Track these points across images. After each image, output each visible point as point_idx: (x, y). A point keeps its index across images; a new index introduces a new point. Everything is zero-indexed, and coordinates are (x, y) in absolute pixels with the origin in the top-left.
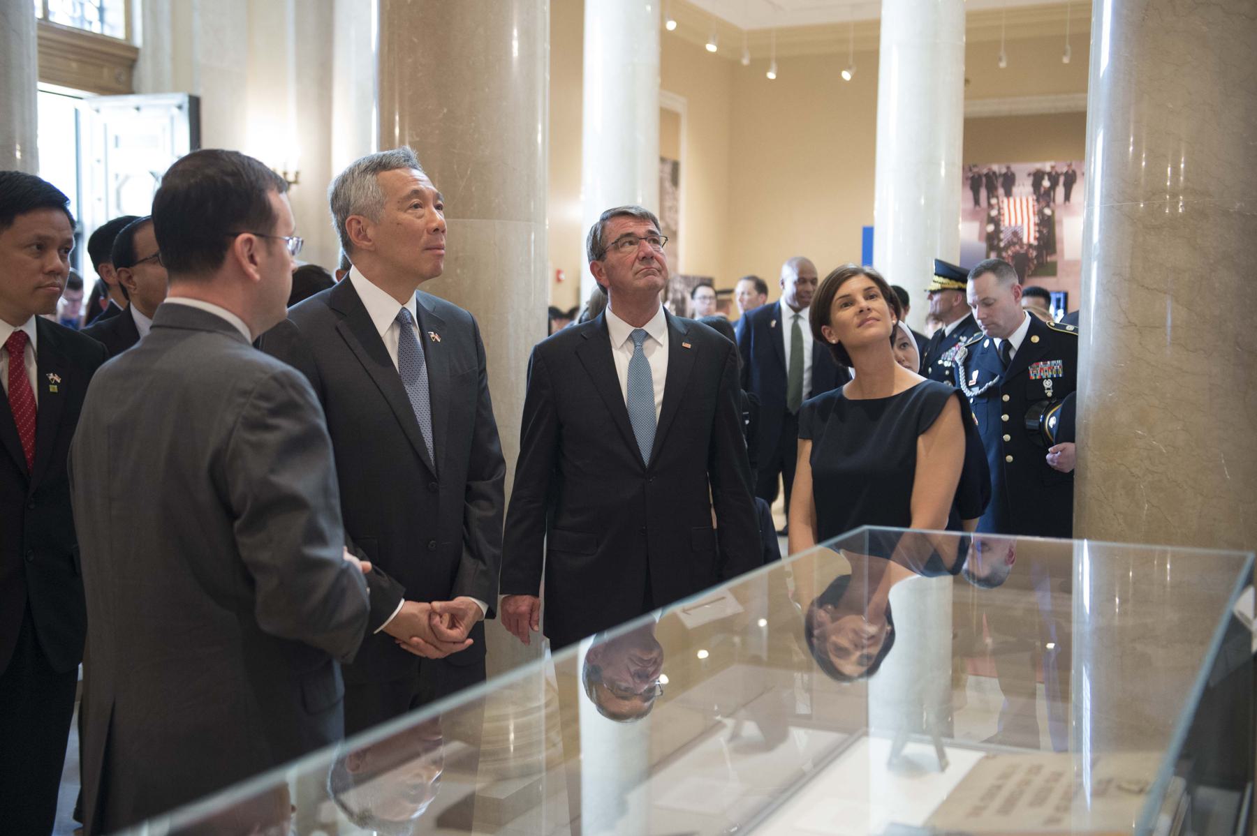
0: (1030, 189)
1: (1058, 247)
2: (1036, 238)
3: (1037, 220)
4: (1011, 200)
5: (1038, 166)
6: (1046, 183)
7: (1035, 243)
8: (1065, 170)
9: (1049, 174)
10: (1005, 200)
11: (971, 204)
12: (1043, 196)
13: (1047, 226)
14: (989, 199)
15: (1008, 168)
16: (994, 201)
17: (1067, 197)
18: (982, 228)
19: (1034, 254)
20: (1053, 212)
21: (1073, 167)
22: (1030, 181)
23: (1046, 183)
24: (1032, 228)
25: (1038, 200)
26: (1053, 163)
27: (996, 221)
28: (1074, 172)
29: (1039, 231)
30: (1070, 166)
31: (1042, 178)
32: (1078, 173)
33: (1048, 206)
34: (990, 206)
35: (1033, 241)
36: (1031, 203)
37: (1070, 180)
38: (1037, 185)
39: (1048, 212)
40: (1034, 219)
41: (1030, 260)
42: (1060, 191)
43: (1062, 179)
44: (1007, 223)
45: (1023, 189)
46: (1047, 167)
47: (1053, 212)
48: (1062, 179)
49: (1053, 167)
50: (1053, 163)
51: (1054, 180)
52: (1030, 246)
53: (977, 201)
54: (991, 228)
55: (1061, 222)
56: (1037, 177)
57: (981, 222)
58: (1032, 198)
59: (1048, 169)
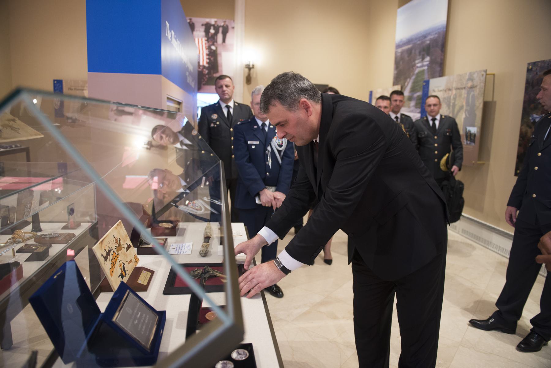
0: (203, 34)
1: (220, 68)
2: (207, 63)
3: (208, 53)
5: (207, 20)
6: (212, 31)
7: (207, 65)
8: (222, 24)
9: (214, 25)
12: (211, 39)
13: (213, 56)
15: (190, 19)
17: (224, 40)
19: (207, 72)
20: (216, 48)
21: (227, 23)
22: (203, 29)
23: (212, 31)
24: (205, 57)
25: (207, 40)
26: (216, 20)
28: (227, 26)
29: (209, 59)
30: (225, 22)
31: (210, 29)
32: (230, 27)
33: (213, 44)
35: (205, 64)
36: (204, 42)
37: (225, 31)
38: (207, 31)
39: (213, 48)
40: (206, 52)
41: (205, 75)
42: (220, 37)
43: (221, 30)
45: (200, 33)
46: (212, 21)
47: (216, 48)
48: (221, 30)
49: (216, 22)
50: (216, 20)
51: (217, 29)
52: (204, 67)
55: (220, 54)
56: (207, 27)
58: (204, 39)
59: (213, 23)
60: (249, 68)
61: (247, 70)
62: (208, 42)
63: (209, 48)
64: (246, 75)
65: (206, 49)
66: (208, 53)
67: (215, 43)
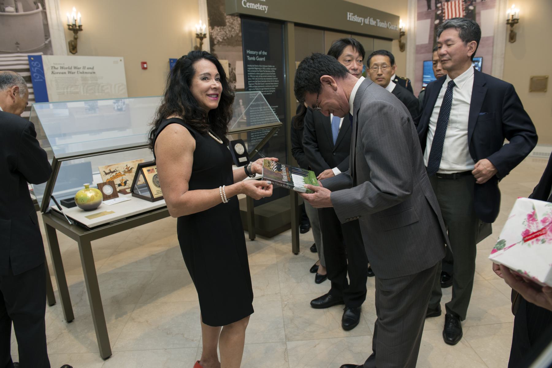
4: (449, 3)
10: (446, 4)
11: (425, 9)
14: (436, 4)
16: (439, 5)
18: (432, 23)
20: (475, 7)
27: (440, 17)
33: (471, 4)
34: (437, 8)
36: (461, 3)
44: (446, 18)
47: (475, 7)
53: (429, 7)
54: (437, 22)
55: (479, 13)
57: (432, 19)
60: (513, 23)
61: (509, 25)
62: (466, 3)
63: (466, 9)
64: (509, 32)
65: (463, 11)
66: (465, 14)
67: (474, 3)
